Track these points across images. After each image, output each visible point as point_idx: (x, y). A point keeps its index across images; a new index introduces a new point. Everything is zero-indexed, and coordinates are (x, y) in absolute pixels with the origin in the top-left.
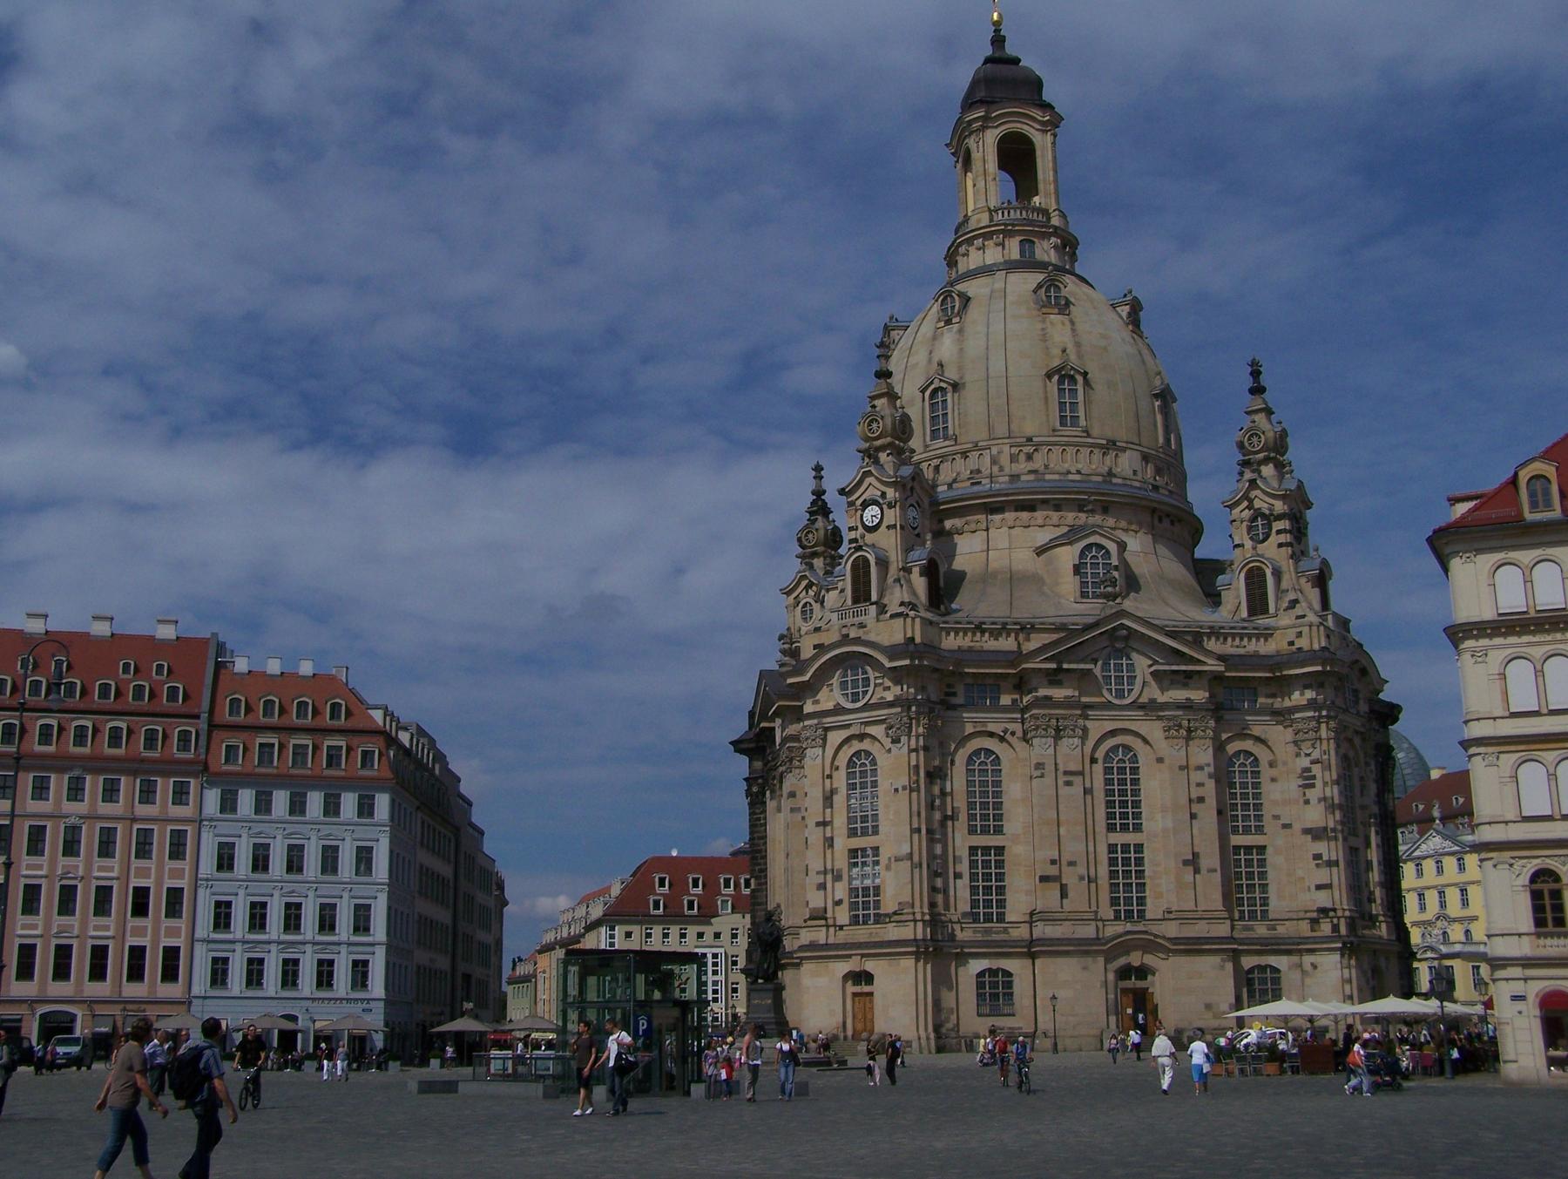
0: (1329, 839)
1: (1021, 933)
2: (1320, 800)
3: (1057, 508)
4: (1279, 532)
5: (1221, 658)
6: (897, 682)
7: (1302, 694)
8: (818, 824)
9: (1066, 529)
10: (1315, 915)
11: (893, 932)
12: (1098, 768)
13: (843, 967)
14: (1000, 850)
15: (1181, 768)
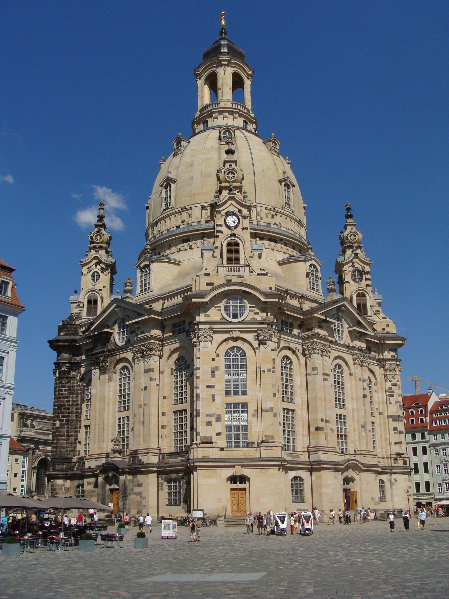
0: (401, 421)
1: (304, 457)
2: (397, 402)
3: (285, 245)
4: (366, 279)
5: (374, 330)
6: (264, 310)
7: (389, 353)
8: (208, 386)
9: (287, 256)
10: (395, 456)
11: (264, 453)
12: (332, 374)
13: (230, 472)
14: (293, 411)
15: (360, 379)
